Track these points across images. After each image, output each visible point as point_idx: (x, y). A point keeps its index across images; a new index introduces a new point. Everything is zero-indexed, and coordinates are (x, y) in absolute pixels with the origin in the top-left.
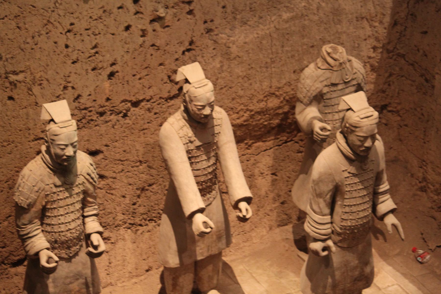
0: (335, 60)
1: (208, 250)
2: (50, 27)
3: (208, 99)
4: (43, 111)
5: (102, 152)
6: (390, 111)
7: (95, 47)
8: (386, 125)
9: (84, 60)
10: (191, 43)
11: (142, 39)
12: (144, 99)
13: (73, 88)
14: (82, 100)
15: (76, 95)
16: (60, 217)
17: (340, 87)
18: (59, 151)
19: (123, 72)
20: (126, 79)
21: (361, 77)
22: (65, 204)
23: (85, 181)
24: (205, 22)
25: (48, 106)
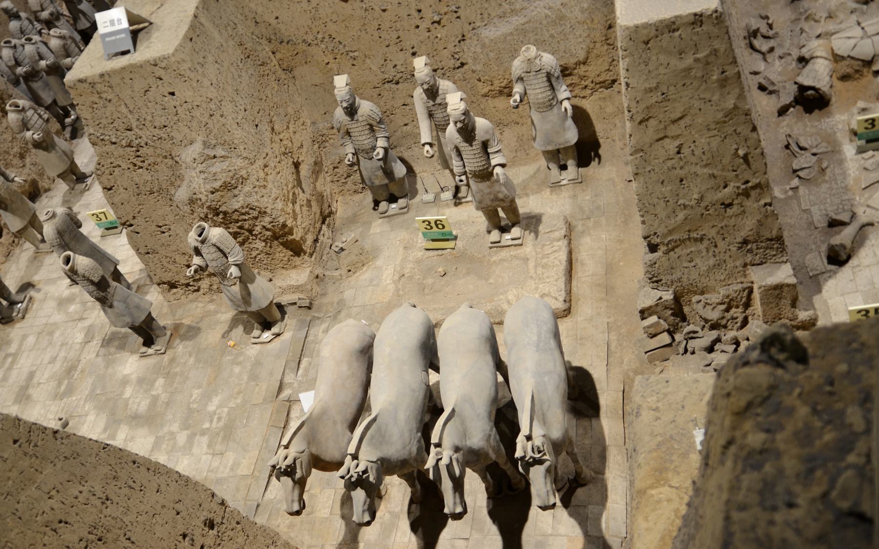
7: (399, 37)
10: (463, 36)
17: (532, 74)
21: (550, 68)
24: (470, 24)
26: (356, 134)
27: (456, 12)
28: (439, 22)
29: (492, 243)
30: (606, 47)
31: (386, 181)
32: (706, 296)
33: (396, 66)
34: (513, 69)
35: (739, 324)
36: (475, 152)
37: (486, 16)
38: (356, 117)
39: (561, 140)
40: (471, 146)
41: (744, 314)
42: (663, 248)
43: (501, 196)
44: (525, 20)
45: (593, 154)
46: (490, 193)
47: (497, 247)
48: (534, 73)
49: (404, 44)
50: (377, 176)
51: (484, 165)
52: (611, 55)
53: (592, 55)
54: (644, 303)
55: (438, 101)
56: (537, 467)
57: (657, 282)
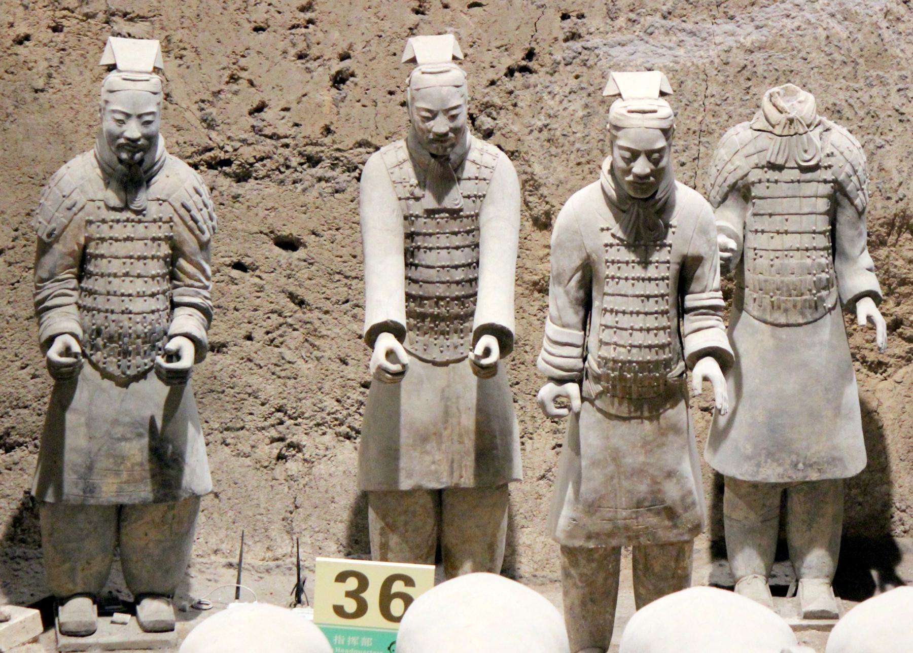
1: (452, 473)
3: (443, 100)
9: (282, 31)
10: (530, 55)
13: (251, 83)
14: (267, 114)
16: (111, 279)
17: (788, 175)
18: (115, 128)
21: (848, 169)
23: (176, 219)
24: (565, 17)
26: (116, 266)
31: (145, 492)
33: (260, 108)
34: (722, 153)
36: (651, 289)
38: (142, 199)
39: (818, 449)
43: (671, 492)
44: (754, 37)
45: (874, 574)
46: (639, 472)
48: (796, 174)
50: (120, 459)
51: (662, 347)
55: (454, 198)
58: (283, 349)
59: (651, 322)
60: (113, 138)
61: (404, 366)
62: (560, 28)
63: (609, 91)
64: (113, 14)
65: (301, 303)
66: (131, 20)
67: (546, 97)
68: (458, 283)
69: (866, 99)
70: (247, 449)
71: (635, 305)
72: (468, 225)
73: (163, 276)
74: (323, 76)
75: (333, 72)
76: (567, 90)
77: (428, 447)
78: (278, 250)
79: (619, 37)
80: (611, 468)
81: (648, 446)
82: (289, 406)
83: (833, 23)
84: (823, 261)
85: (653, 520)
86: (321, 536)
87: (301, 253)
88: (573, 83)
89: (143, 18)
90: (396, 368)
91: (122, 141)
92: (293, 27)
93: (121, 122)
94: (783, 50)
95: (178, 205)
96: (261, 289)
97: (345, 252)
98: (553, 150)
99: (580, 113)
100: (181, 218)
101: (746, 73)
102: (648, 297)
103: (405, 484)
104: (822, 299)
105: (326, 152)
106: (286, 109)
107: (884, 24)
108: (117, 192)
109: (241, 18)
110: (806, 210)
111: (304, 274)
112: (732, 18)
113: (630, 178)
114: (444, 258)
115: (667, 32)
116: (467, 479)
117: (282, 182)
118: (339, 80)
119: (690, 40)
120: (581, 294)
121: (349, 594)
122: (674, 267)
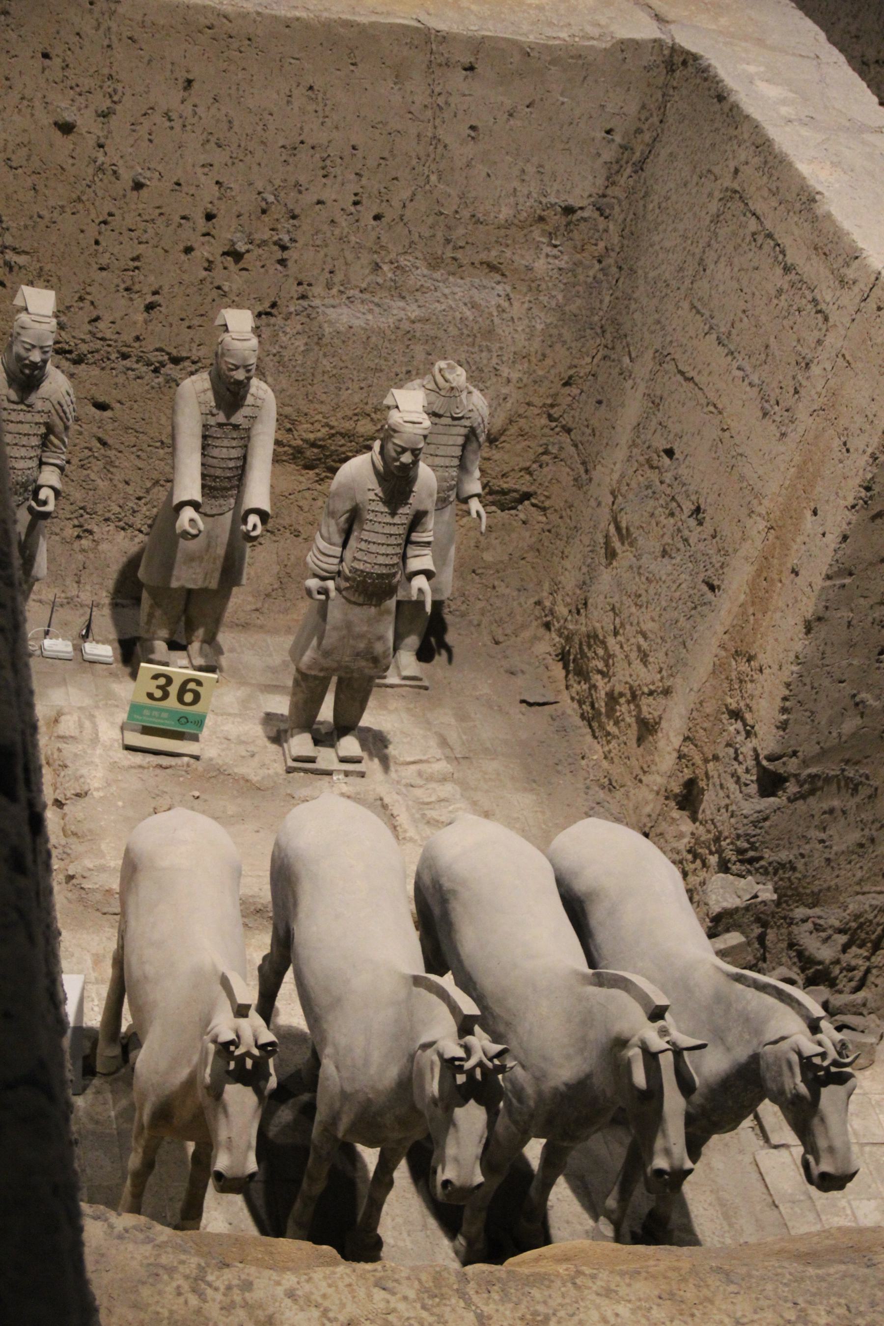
0: (446, 381)
1: (205, 579)
2: (80, 206)
3: (245, 359)
4: (19, 293)
5: (112, 409)
6: (534, 505)
8: (524, 523)
9: (117, 272)
10: (274, 305)
11: (205, 273)
12: (188, 358)
13: (92, 303)
14: (101, 325)
15: (94, 316)
18: (23, 353)
19: (167, 307)
20: (170, 319)
21: (480, 420)
22: (16, 431)
23: (53, 411)
24: (300, 284)
25: (26, 290)
27: (284, 248)
28: (237, 256)
29: (296, 760)
30: (544, 421)
32: (817, 911)
33: (97, 319)
35: (853, 984)
36: (394, 530)
37: (338, 277)
38: (33, 398)
40: (393, 514)
41: (867, 964)
42: (792, 788)
46: (361, 636)
47: (306, 771)
48: (448, 421)
49: (142, 278)
51: (393, 565)
52: (544, 440)
53: (513, 430)
54: (726, 900)
55: (238, 418)
56: (832, 1088)
57: (751, 861)
58: (89, 472)
59: (390, 550)
60: (19, 358)
61: (200, 531)
62: (295, 290)
63: (388, 401)
64: (6, 248)
65: (104, 444)
66: (18, 253)
67: (281, 334)
68: (230, 469)
69: (478, 359)
70: (57, 530)
71: (382, 539)
72: (243, 434)
73: (38, 446)
74: (140, 303)
75: (147, 302)
76: (295, 331)
77: (194, 564)
78: (94, 409)
79: (331, 301)
80: (344, 632)
81: (370, 622)
82: (89, 506)
83: (465, 309)
84: (455, 474)
85: (363, 663)
86: (97, 587)
87: (108, 414)
88: (299, 327)
89: (27, 253)
90: (194, 532)
91: (27, 362)
92: (125, 270)
93: (28, 350)
94: (433, 324)
95: (55, 403)
96: (81, 433)
97: (139, 416)
98: (281, 369)
99: (302, 348)
100: (56, 411)
101: (409, 336)
102: (391, 535)
103: (174, 584)
104: (449, 496)
105: (134, 352)
106: (113, 323)
107: (495, 314)
108: (16, 391)
109: (92, 261)
110: (451, 443)
111: (110, 427)
112: (404, 298)
113: (397, 464)
114: (224, 453)
115: (362, 302)
116: (214, 584)
117: (103, 369)
118: (150, 307)
119: (377, 310)
120: (346, 526)
121: (158, 687)
122: (411, 517)
